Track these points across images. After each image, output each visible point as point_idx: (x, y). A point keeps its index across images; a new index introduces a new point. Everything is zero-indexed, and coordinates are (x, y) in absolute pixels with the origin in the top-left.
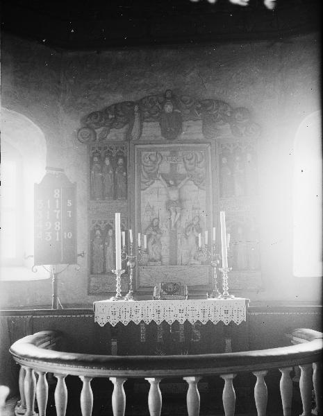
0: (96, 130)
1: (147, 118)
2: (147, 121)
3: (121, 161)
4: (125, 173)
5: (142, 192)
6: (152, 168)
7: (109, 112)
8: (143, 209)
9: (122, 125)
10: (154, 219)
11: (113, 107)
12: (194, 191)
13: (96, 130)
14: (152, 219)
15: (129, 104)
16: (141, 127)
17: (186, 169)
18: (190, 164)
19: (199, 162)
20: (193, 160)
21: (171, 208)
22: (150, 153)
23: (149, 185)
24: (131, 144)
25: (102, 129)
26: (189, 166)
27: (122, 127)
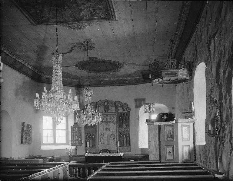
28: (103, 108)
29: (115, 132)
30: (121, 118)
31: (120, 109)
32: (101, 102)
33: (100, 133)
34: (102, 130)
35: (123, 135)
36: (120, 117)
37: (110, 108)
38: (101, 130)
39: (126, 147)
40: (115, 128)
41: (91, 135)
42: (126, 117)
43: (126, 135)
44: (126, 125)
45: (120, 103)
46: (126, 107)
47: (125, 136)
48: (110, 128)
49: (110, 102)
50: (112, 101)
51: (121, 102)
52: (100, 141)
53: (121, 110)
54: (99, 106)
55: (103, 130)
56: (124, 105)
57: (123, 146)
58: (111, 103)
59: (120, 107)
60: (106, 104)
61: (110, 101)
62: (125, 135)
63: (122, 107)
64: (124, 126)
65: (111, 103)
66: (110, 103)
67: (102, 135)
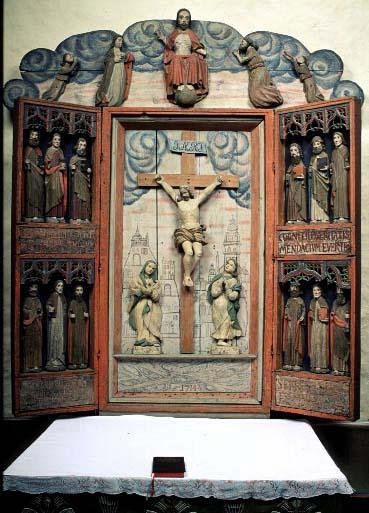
0: (39, 86)
1: (140, 63)
2: (141, 71)
3: (82, 145)
4: (89, 170)
5: (126, 208)
6: (145, 161)
7: (65, 51)
8: (126, 241)
9: (90, 75)
10: (147, 264)
11: (75, 38)
12: (230, 209)
13: (39, 86)
14: (143, 263)
15: (104, 35)
16: (127, 83)
17: (215, 167)
18: (223, 156)
19: (241, 154)
20: (227, 150)
21: (187, 246)
22: (143, 132)
23: (139, 196)
24: (107, 117)
25: (50, 83)
26: (221, 162)
27: (91, 80)
28: (160, 75)
29: (245, 262)
30: (295, 150)
31: (290, 86)
32: (146, 33)
33: (132, 262)
34: (146, 242)
35: (305, 290)
36: (287, 142)
37: (214, 77)
38: (140, 240)
39: (316, 382)
40: (246, 231)
41: (62, 278)
42: (330, 146)
43: (329, 290)
44: (330, 212)
45: (288, 48)
46: (332, 77)
47: (317, 291)
48: (208, 230)
49: (213, 35)
50: (230, 31)
51: (293, 41)
52: (126, 317)
53: (293, 95)
54: (129, 63)
55: (152, 241)
56: (316, 65)
57: (306, 364)
58: (224, 47)
59: (287, 75)
60: (183, 41)
61: (212, 28)
62: (323, 285)
63: (297, 73)
64: (318, 213)
65: (224, 47)
66: (212, 42)
67: (144, 272)
